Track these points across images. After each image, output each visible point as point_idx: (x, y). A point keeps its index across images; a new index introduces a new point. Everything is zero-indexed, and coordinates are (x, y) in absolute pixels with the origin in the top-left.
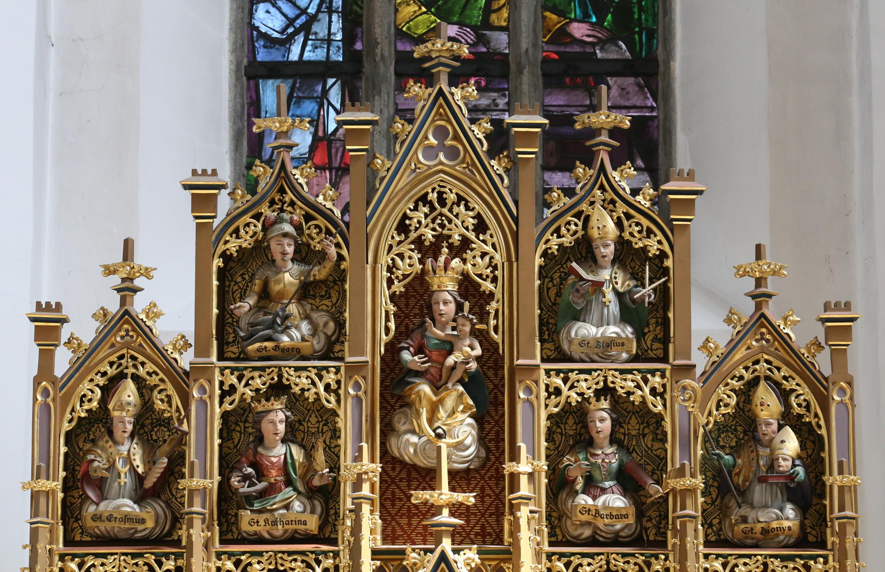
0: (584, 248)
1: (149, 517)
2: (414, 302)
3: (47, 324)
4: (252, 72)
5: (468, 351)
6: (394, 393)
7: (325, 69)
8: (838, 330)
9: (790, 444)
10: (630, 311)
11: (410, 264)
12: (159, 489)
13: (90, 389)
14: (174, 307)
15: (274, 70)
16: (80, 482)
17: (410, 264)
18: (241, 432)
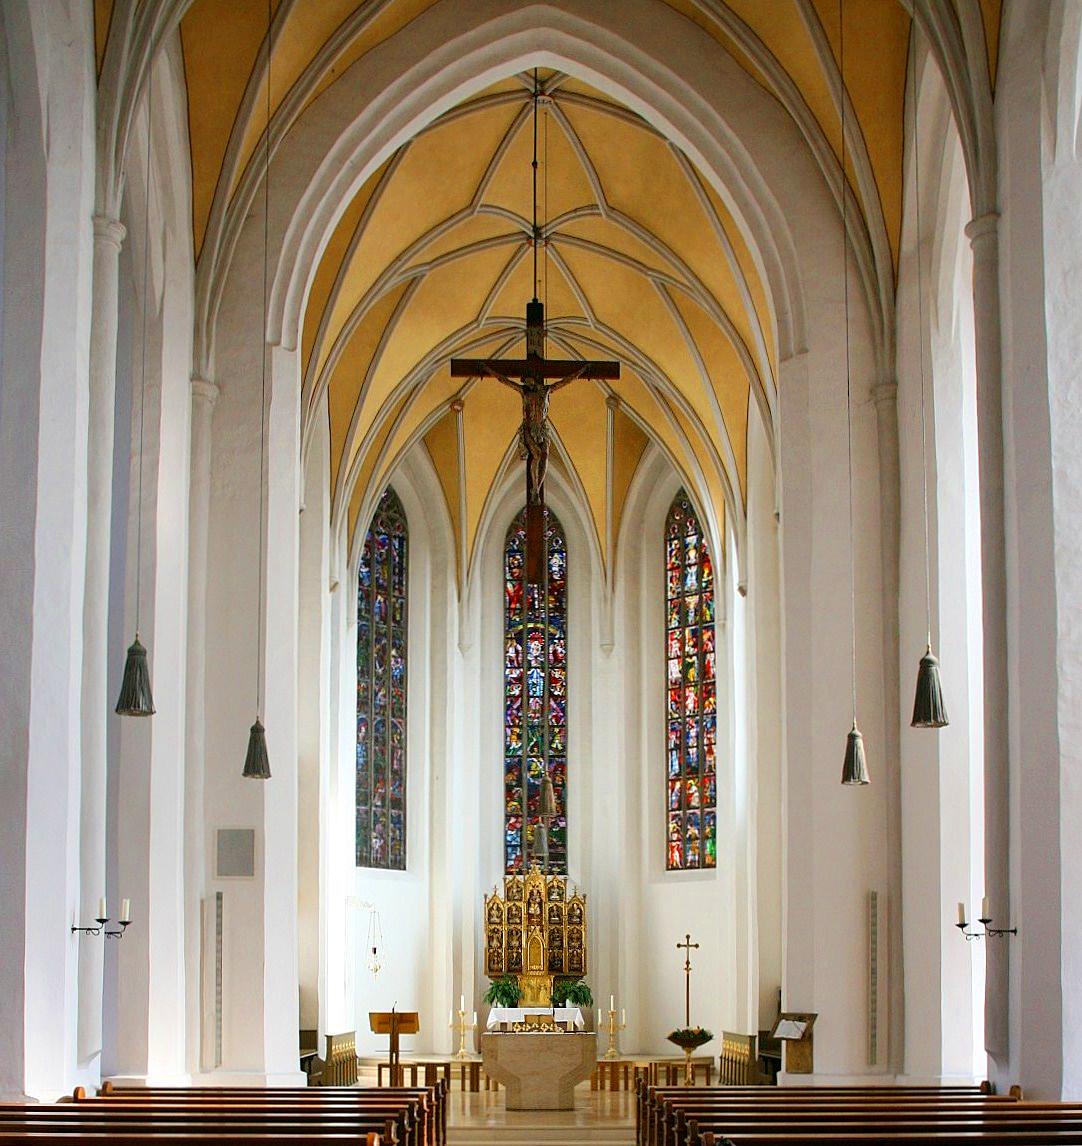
0: (553, 886)
1: (498, 920)
2: (532, 893)
3: (486, 896)
4: (507, 846)
5: (538, 900)
6: (529, 905)
7: (517, 846)
8: (585, 897)
9: (578, 911)
10: (559, 894)
11: (531, 888)
12: (500, 917)
13: (491, 905)
14: (501, 894)
15: (511, 846)
16: (490, 915)
17: (531, 888)
18: (510, 909)
